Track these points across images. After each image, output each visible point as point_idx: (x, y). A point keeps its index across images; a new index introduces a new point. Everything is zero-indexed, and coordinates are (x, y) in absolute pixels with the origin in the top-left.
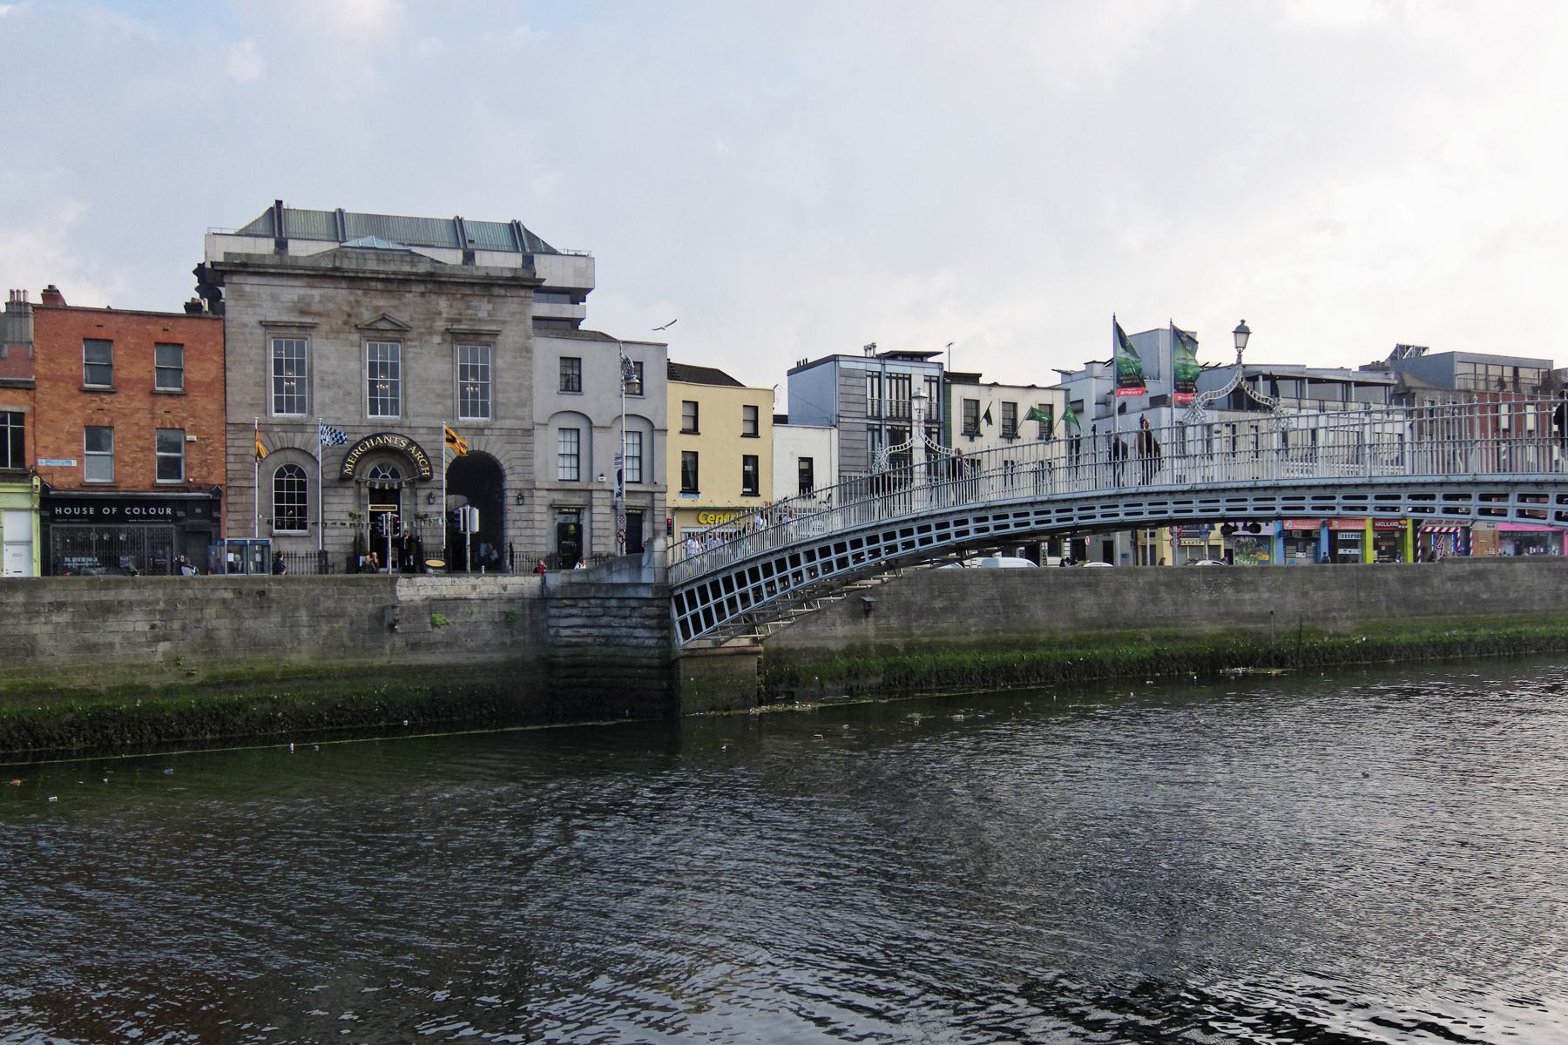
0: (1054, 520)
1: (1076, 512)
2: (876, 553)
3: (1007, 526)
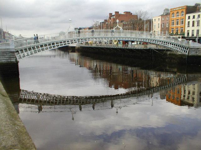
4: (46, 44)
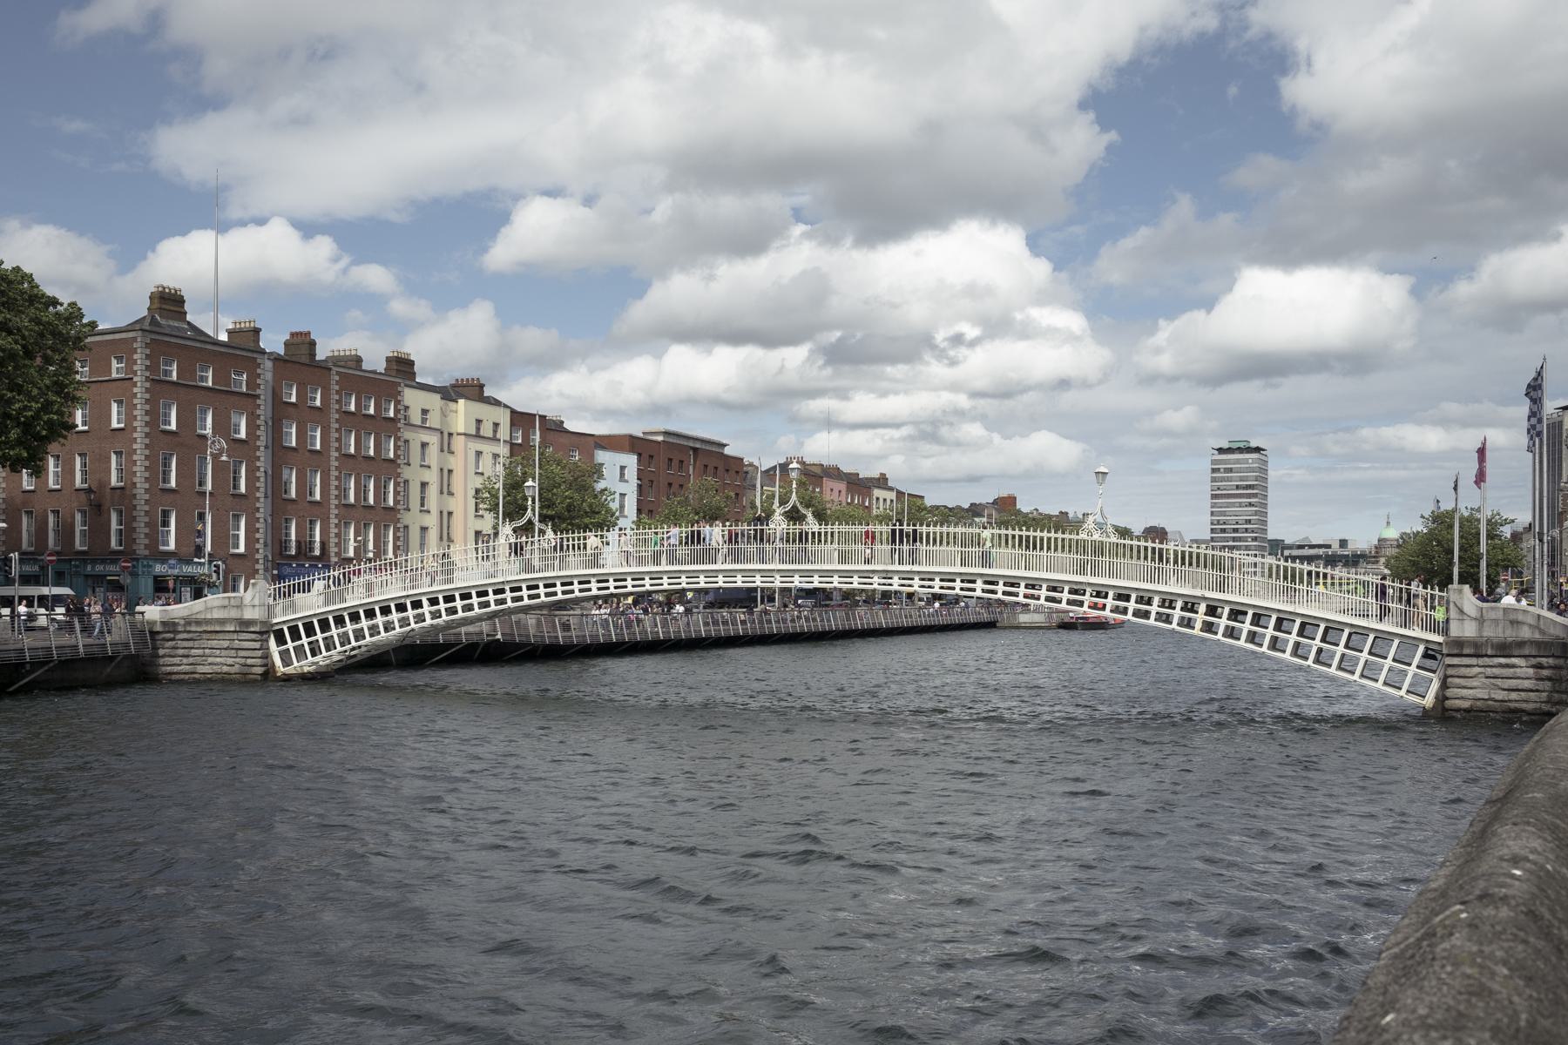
0: (630, 586)
1: (720, 577)
2: (486, 605)
3: (608, 588)
4: (402, 601)
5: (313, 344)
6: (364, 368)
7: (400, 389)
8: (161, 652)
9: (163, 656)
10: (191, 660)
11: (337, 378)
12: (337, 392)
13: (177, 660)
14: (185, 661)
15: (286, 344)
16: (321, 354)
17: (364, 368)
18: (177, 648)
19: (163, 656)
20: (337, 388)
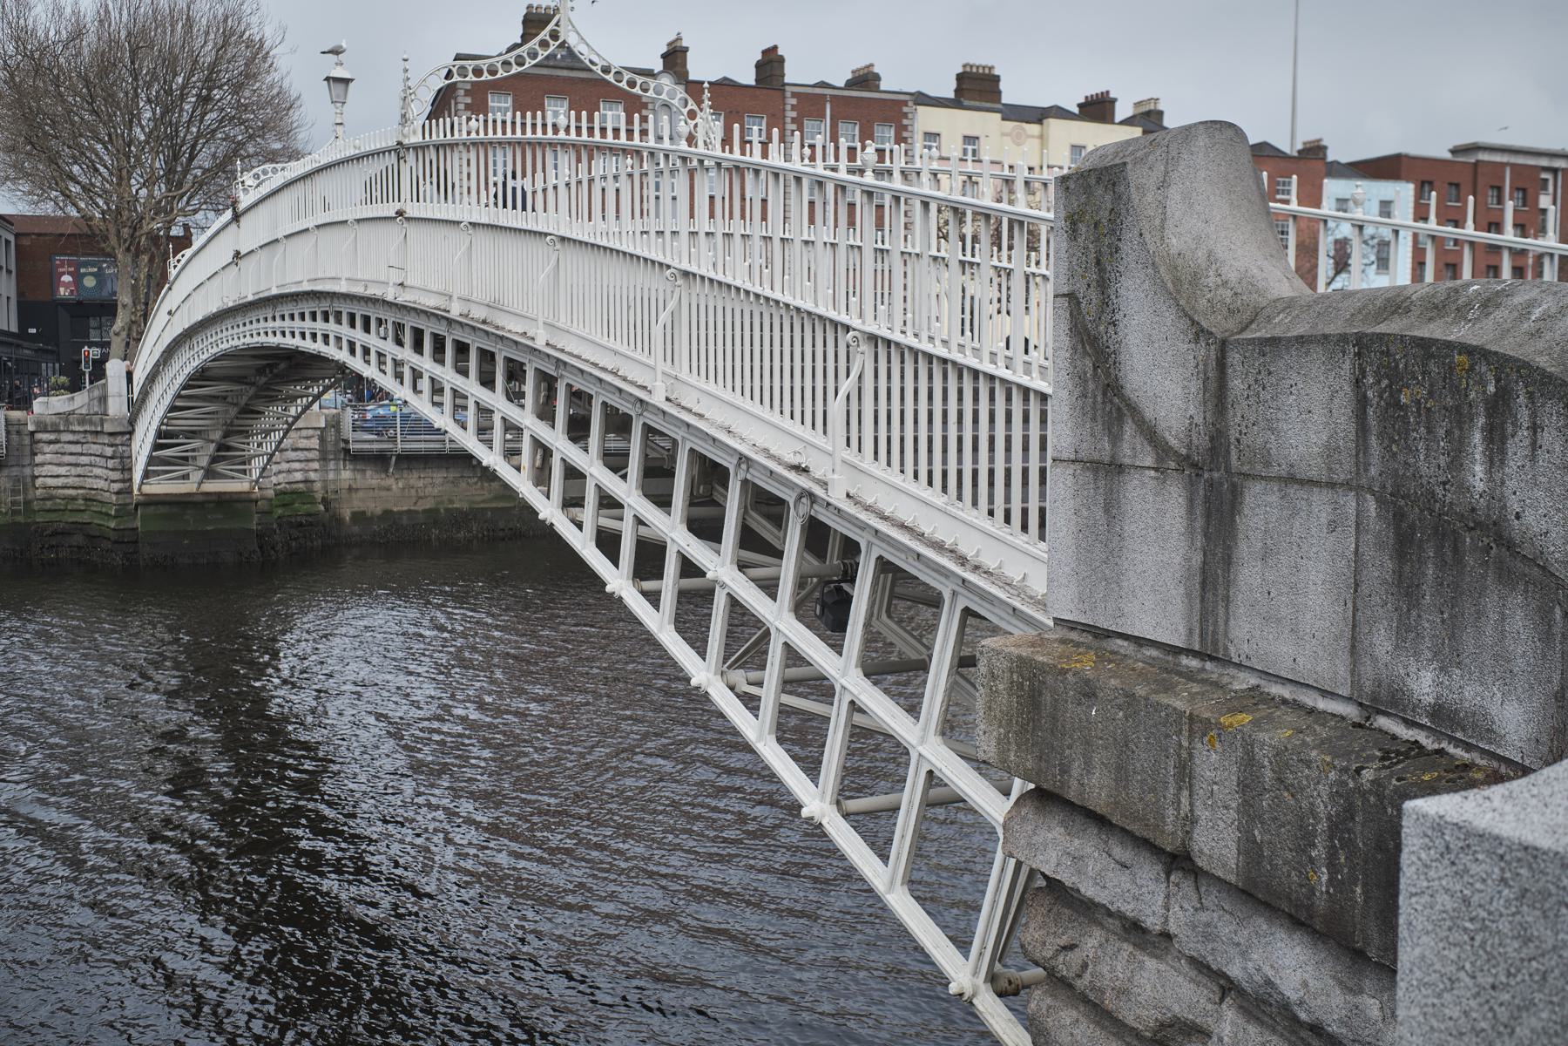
5: (781, 60)
6: (882, 88)
7: (905, 109)
8: (38, 459)
9: (42, 464)
10: (79, 470)
11: (794, 101)
12: (794, 120)
13: (62, 470)
14: (74, 471)
15: (759, 66)
16: (793, 74)
17: (882, 88)
18: (64, 454)
19: (42, 464)
20: (794, 114)
